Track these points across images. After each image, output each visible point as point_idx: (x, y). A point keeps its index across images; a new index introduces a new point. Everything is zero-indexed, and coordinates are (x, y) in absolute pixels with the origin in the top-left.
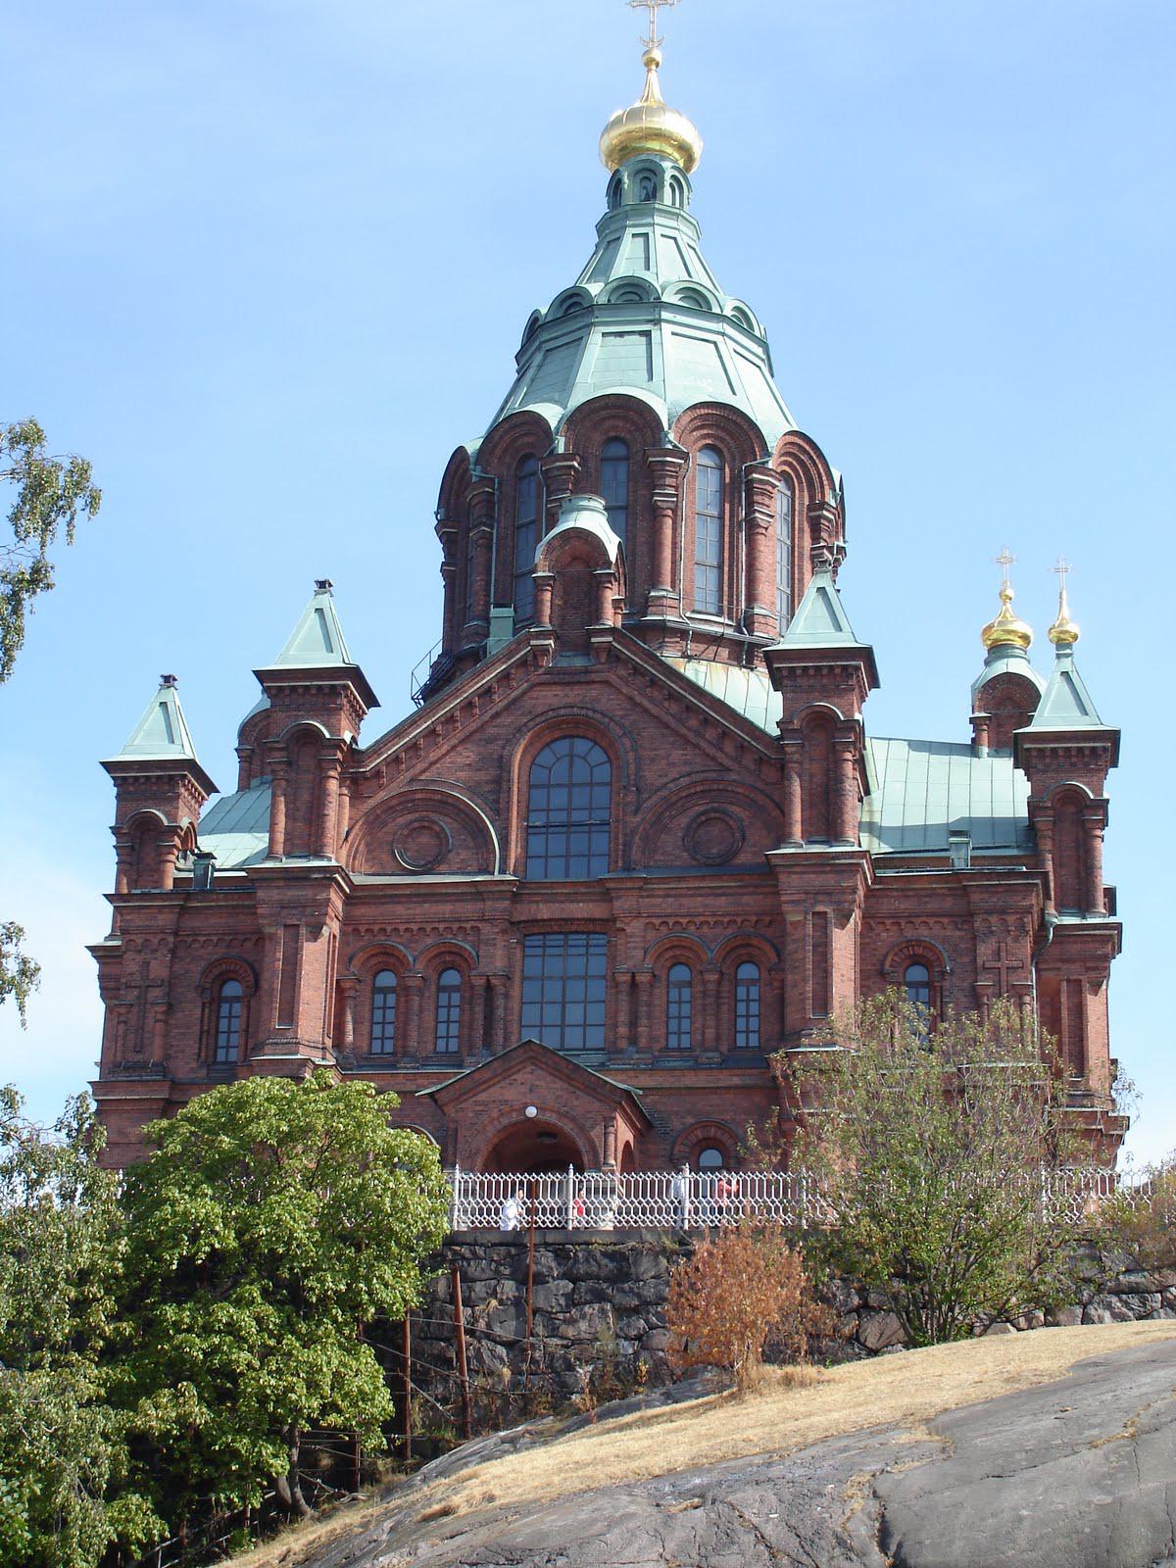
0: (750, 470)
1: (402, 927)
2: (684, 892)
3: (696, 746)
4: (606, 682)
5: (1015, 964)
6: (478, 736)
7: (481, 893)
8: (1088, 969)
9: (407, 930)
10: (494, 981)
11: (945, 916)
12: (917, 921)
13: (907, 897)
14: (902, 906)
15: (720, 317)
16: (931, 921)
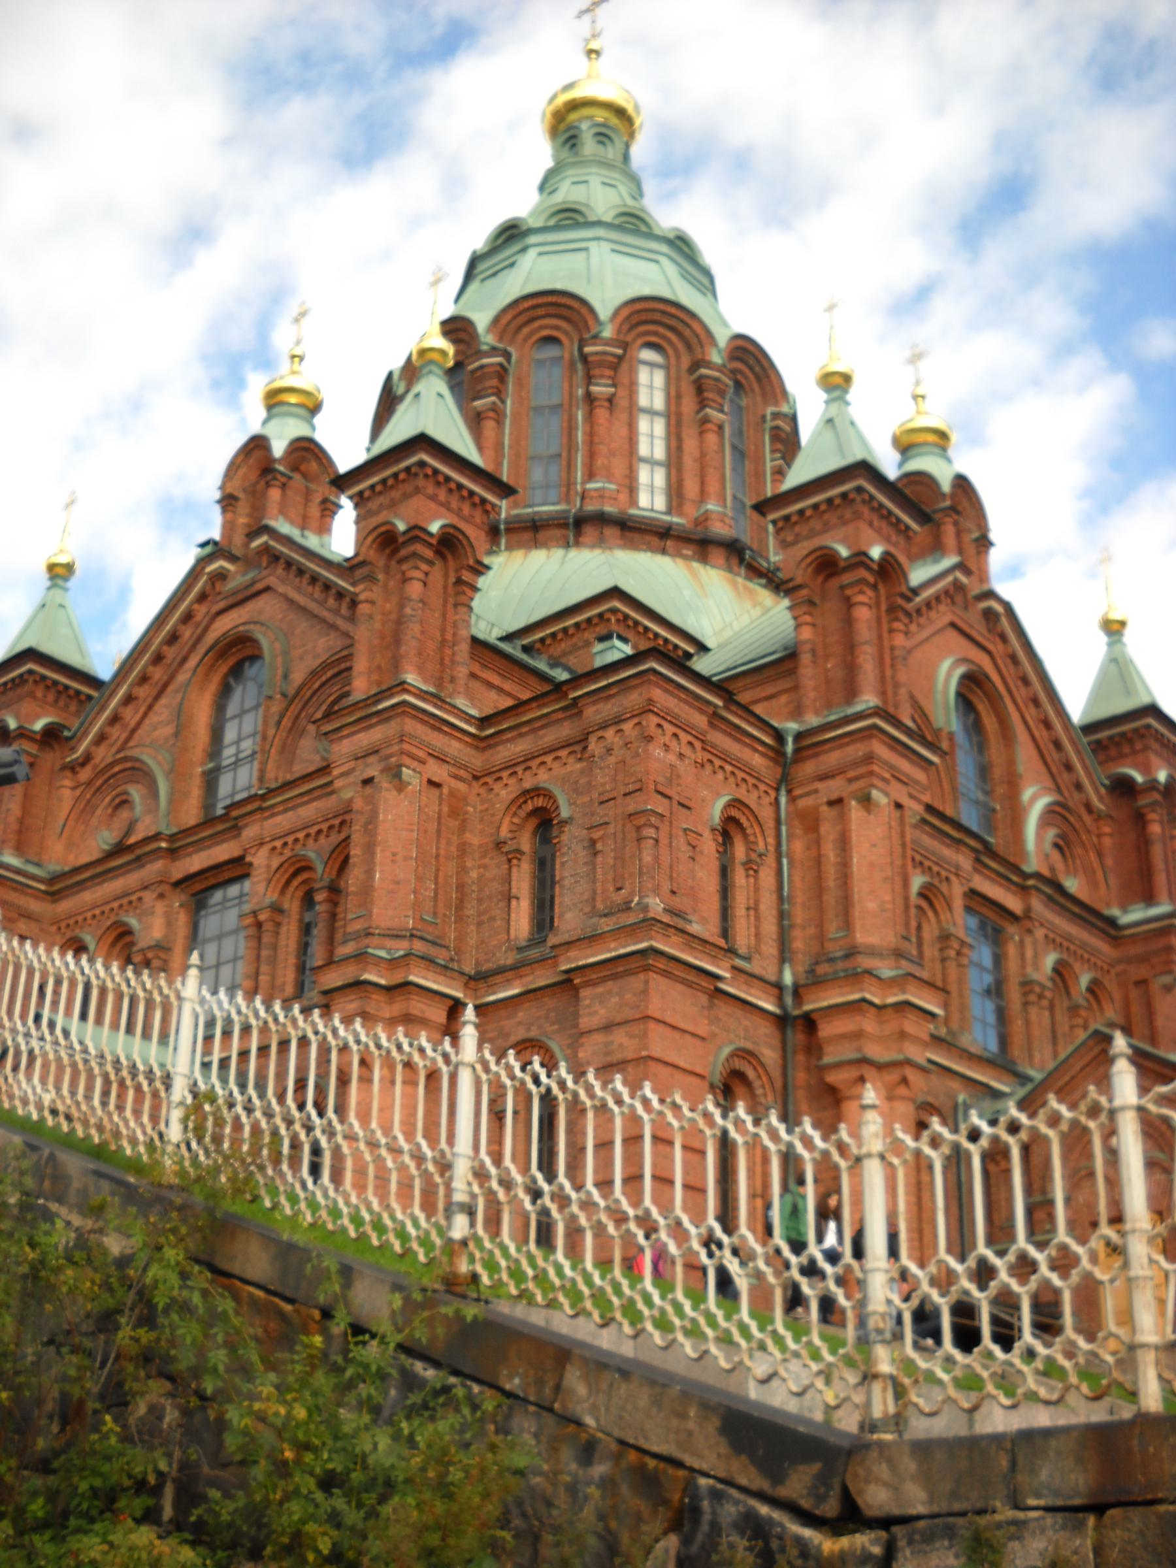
0: (582, 343)
1: (89, 915)
2: (299, 801)
3: (333, 627)
4: (268, 589)
5: (631, 788)
6: (171, 688)
7: (138, 858)
8: (850, 781)
9: (94, 916)
10: (150, 955)
11: (563, 747)
12: (534, 764)
13: (521, 735)
14: (518, 749)
15: (599, 223)
16: (548, 759)
